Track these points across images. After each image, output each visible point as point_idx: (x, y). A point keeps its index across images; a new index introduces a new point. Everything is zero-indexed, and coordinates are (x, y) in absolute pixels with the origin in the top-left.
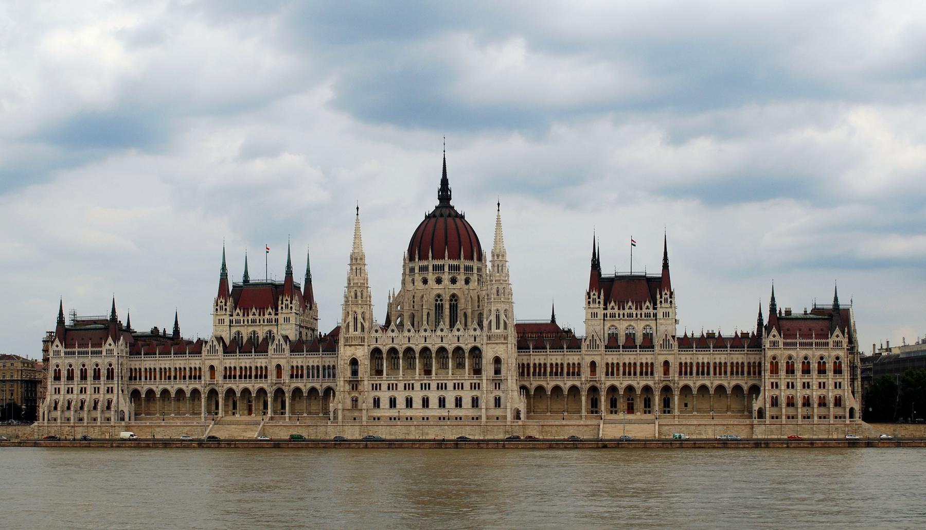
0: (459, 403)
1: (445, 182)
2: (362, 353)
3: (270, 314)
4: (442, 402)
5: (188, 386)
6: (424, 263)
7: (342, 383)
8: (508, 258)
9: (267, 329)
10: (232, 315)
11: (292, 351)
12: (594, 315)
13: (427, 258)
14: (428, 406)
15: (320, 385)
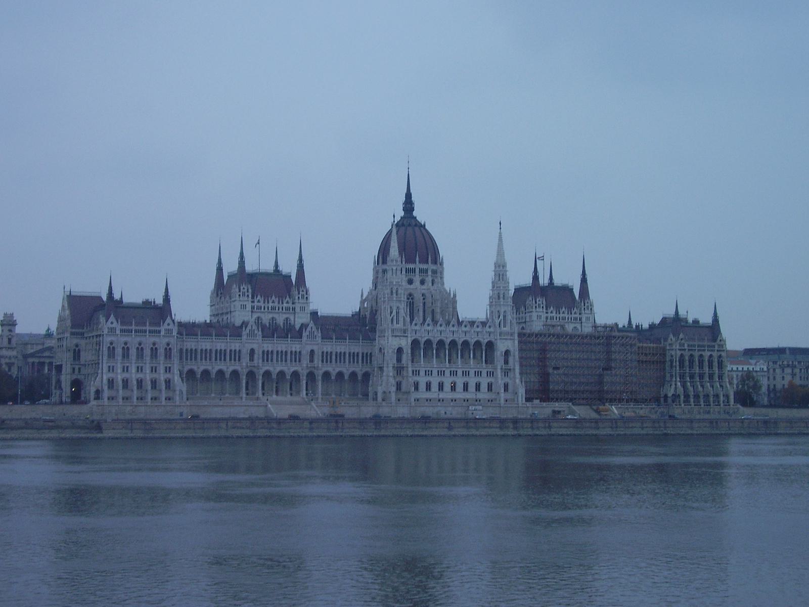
0: (478, 387)
1: (408, 195)
2: (405, 343)
3: (287, 302)
4: (466, 387)
5: (228, 367)
6: (411, 266)
7: (391, 369)
8: (508, 267)
9: (285, 316)
10: (253, 302)
11: (322, 338)
12: (539, 317)
13: (415, 262)
14: (455, 390)
15: (347, 369)
